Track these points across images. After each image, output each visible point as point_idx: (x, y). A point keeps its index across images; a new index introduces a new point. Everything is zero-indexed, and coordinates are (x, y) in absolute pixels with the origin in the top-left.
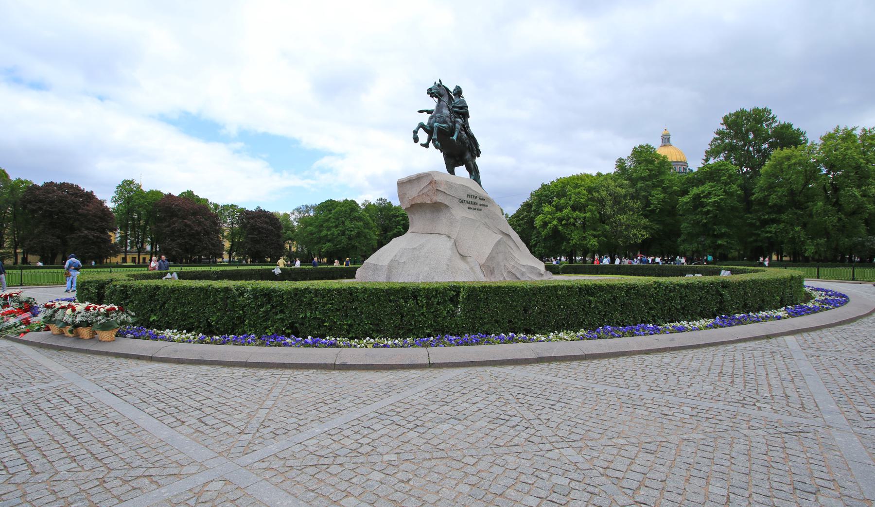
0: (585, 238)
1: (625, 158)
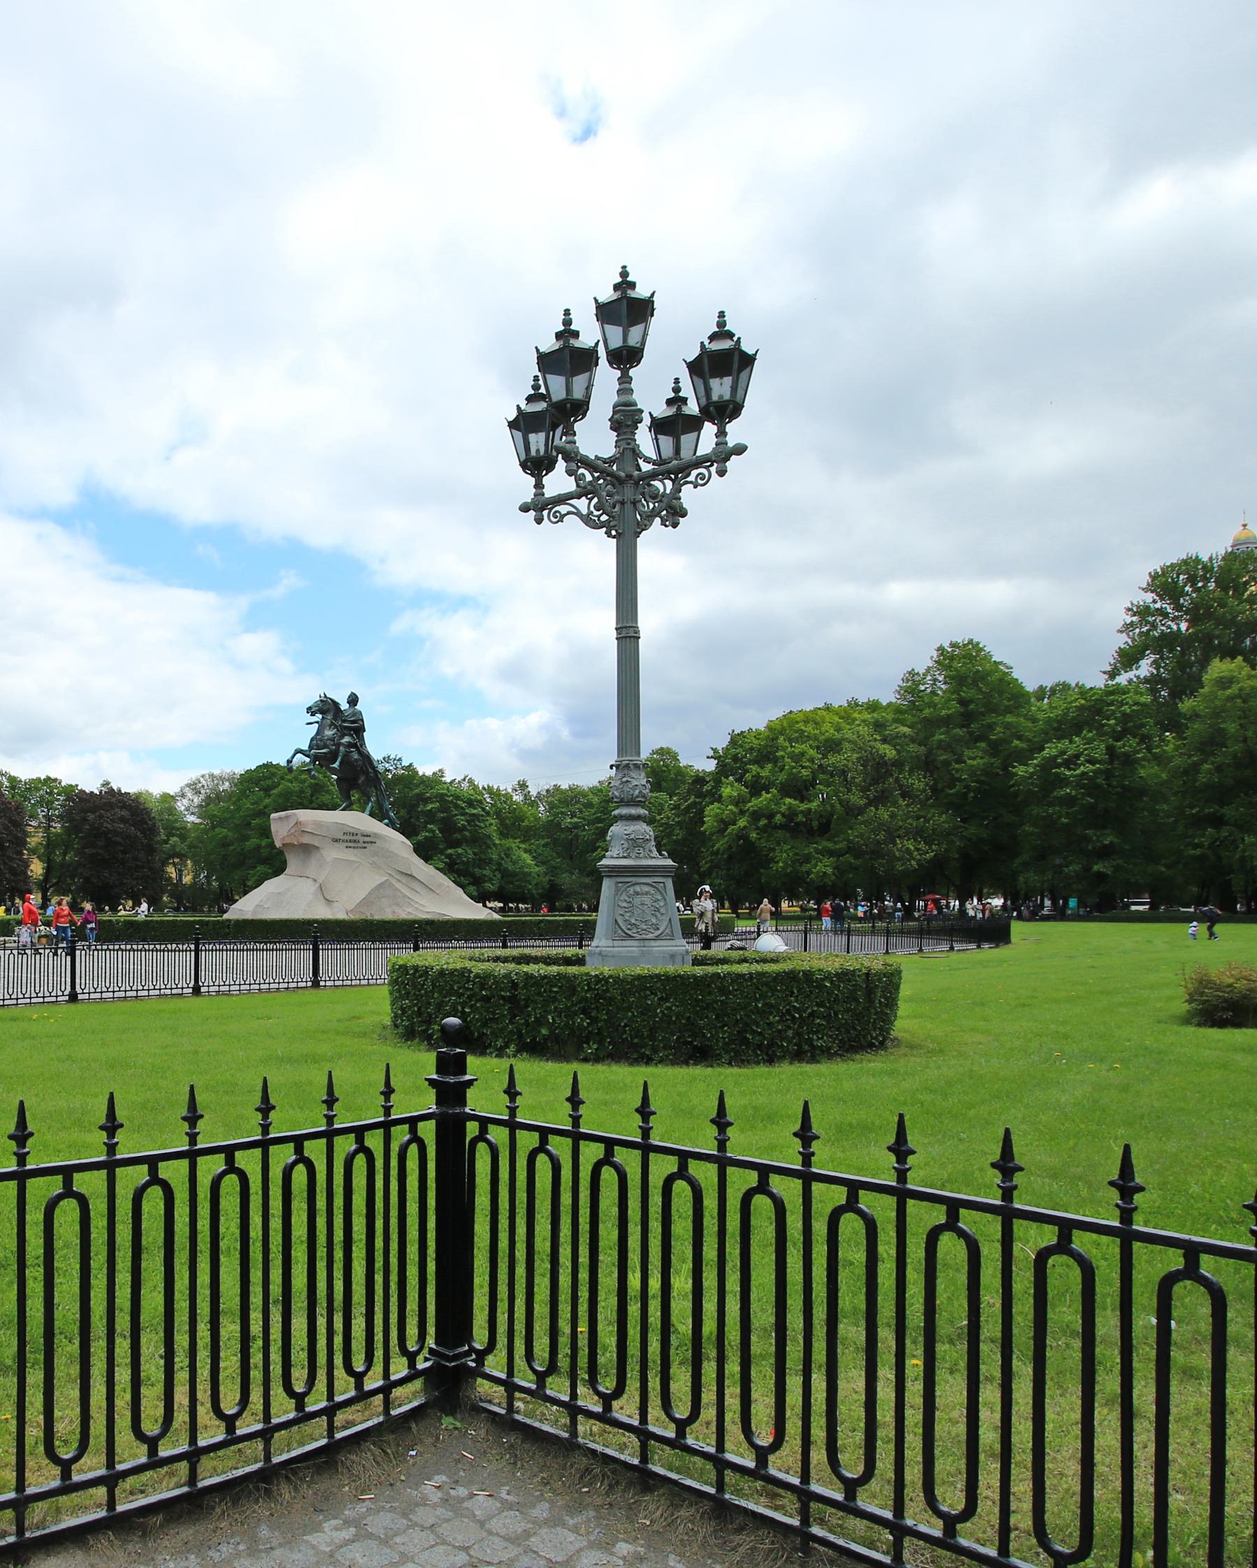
0: (808, 859)
1: (921, 670)
